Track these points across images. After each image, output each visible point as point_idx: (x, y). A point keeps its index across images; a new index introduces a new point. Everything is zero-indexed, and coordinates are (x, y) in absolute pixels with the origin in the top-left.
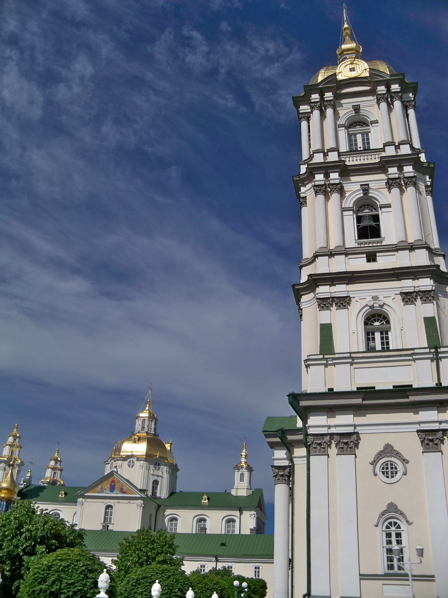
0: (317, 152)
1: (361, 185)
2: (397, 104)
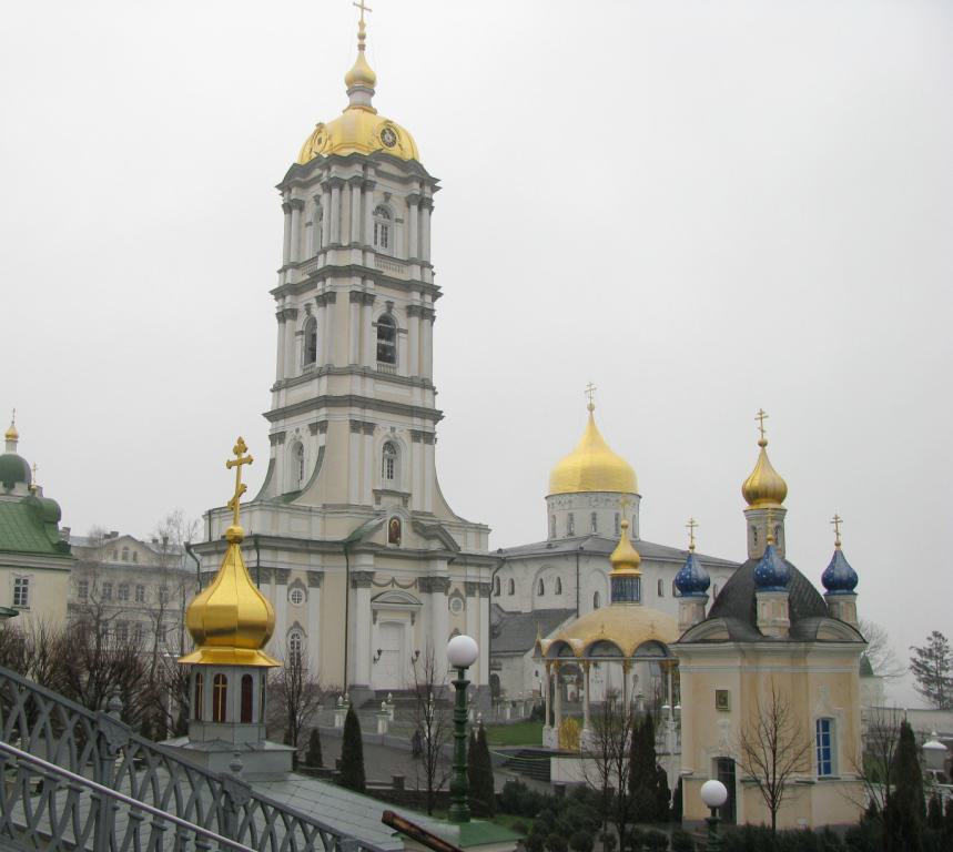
2: (426, 211)
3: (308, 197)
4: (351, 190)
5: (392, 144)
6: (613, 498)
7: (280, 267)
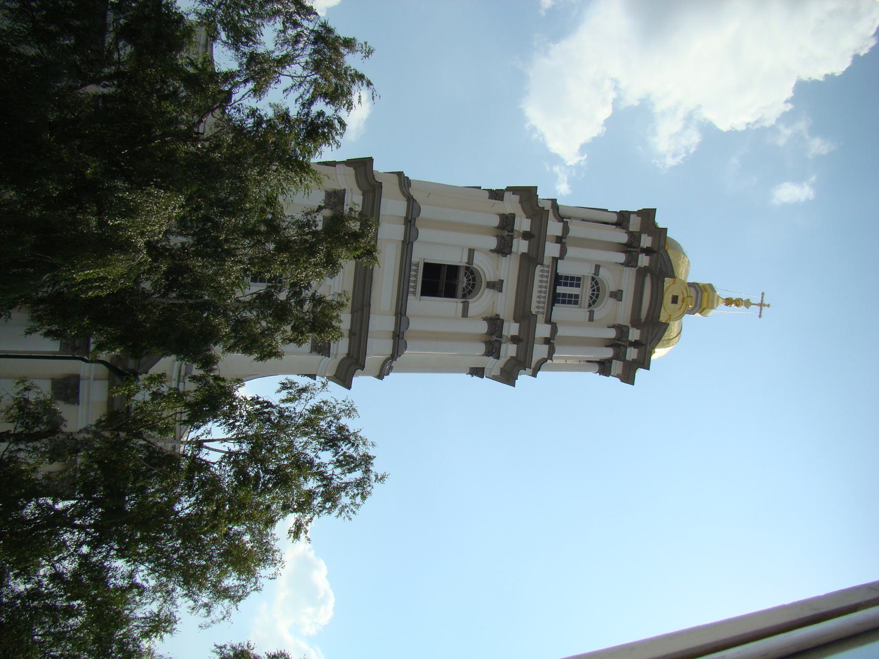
0: (566, 229)
1: (502, 281)
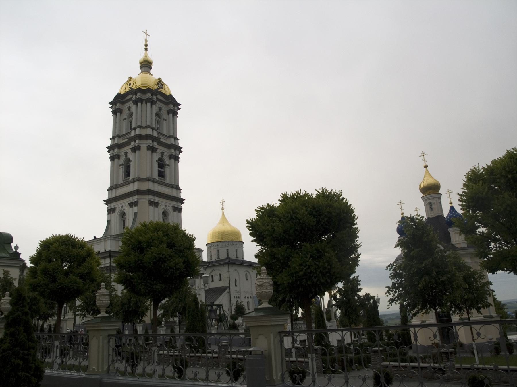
2: (175, 117)
3: (125, 107)
4: (146, 104)
5: (162, 88)
6: (234, 243)
7: (111, 137)
